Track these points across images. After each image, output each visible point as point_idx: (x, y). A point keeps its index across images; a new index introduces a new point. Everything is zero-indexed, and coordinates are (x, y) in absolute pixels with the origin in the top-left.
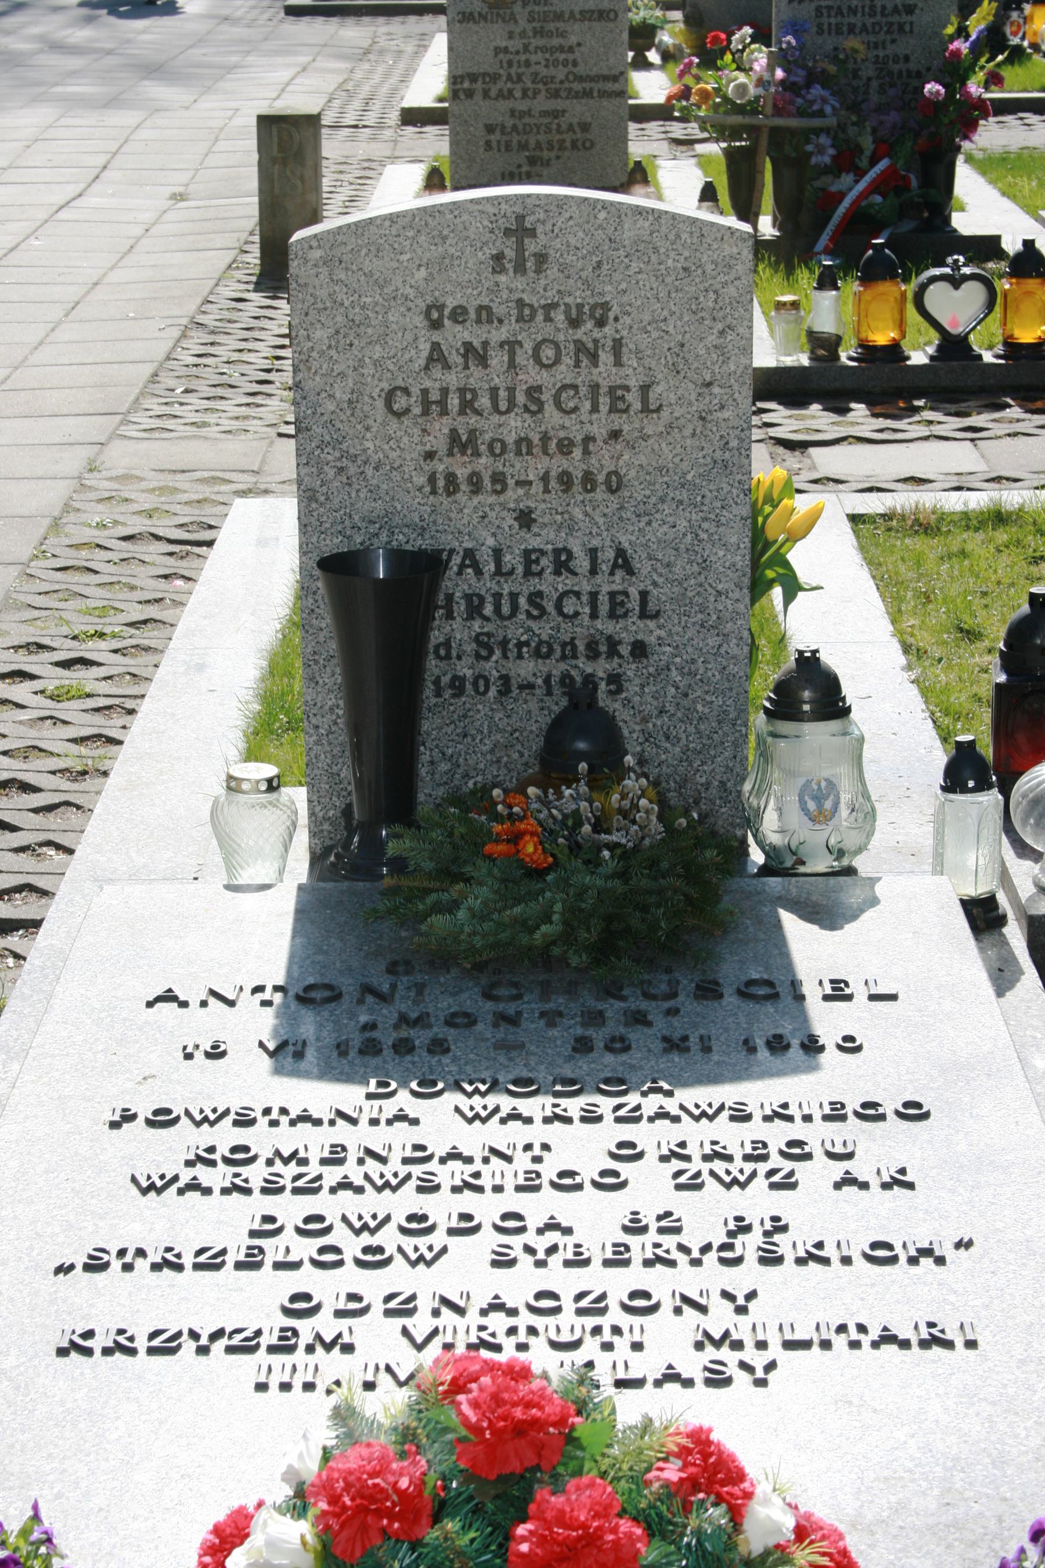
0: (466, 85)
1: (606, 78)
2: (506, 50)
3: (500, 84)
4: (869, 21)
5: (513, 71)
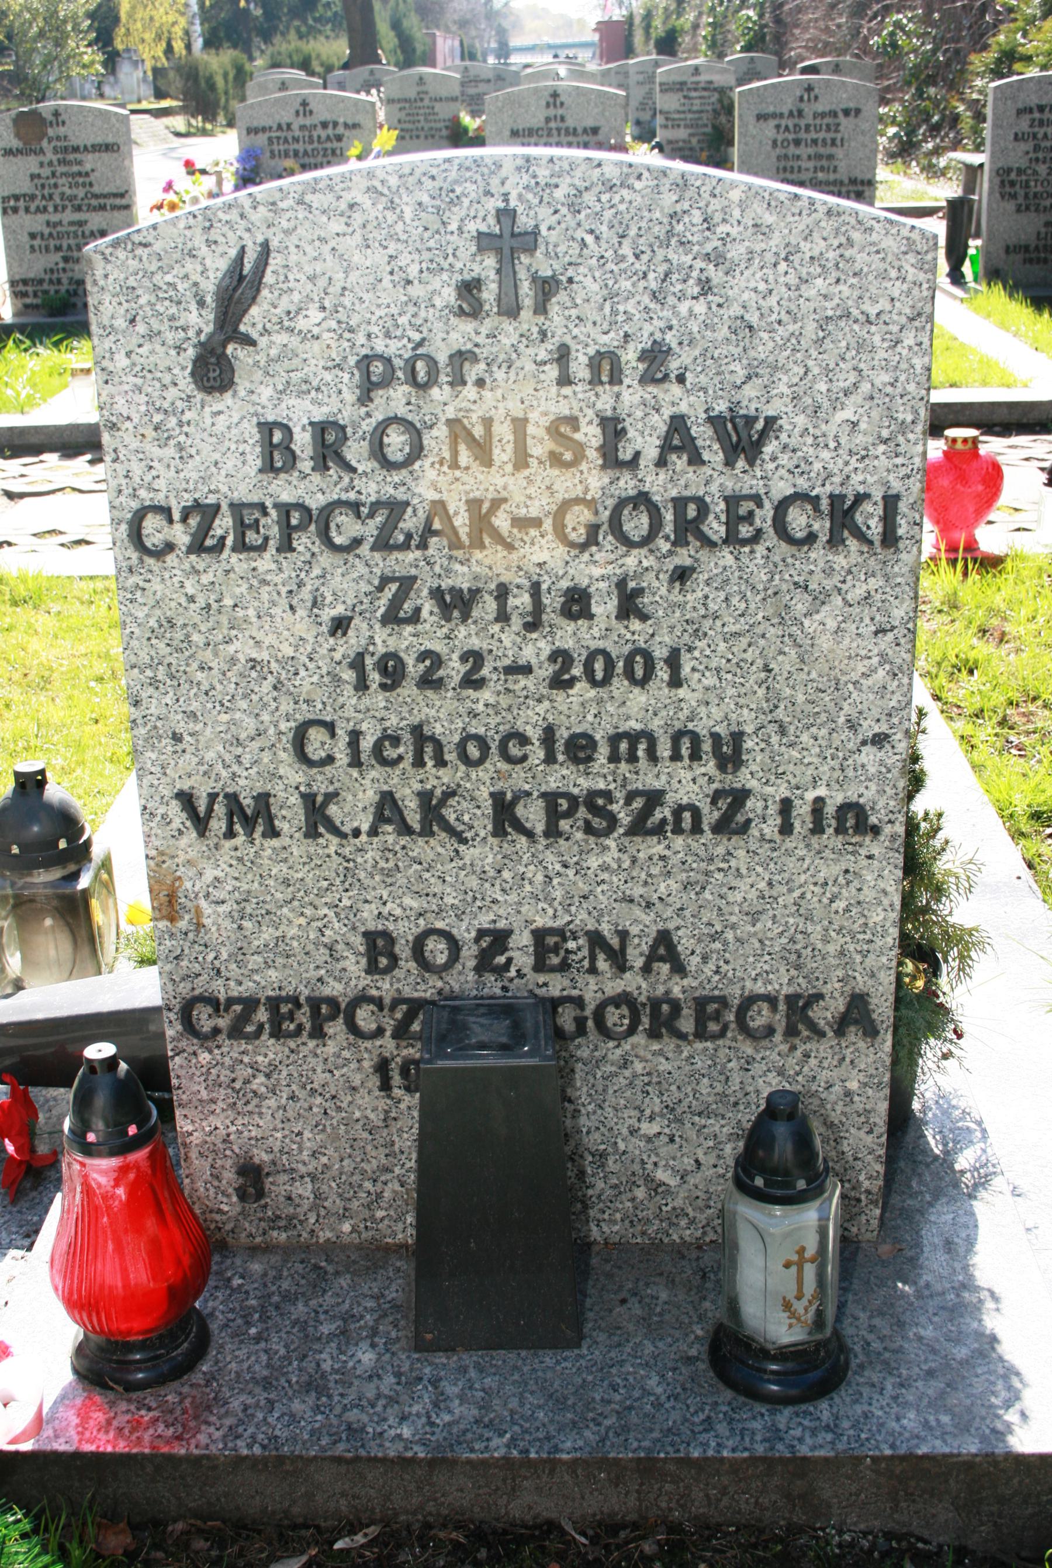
0: (12, 203)
1: (115, 195)
2: (39, 176)
3: (37, 202)
4: (309, 148)
5: (46, 192)
